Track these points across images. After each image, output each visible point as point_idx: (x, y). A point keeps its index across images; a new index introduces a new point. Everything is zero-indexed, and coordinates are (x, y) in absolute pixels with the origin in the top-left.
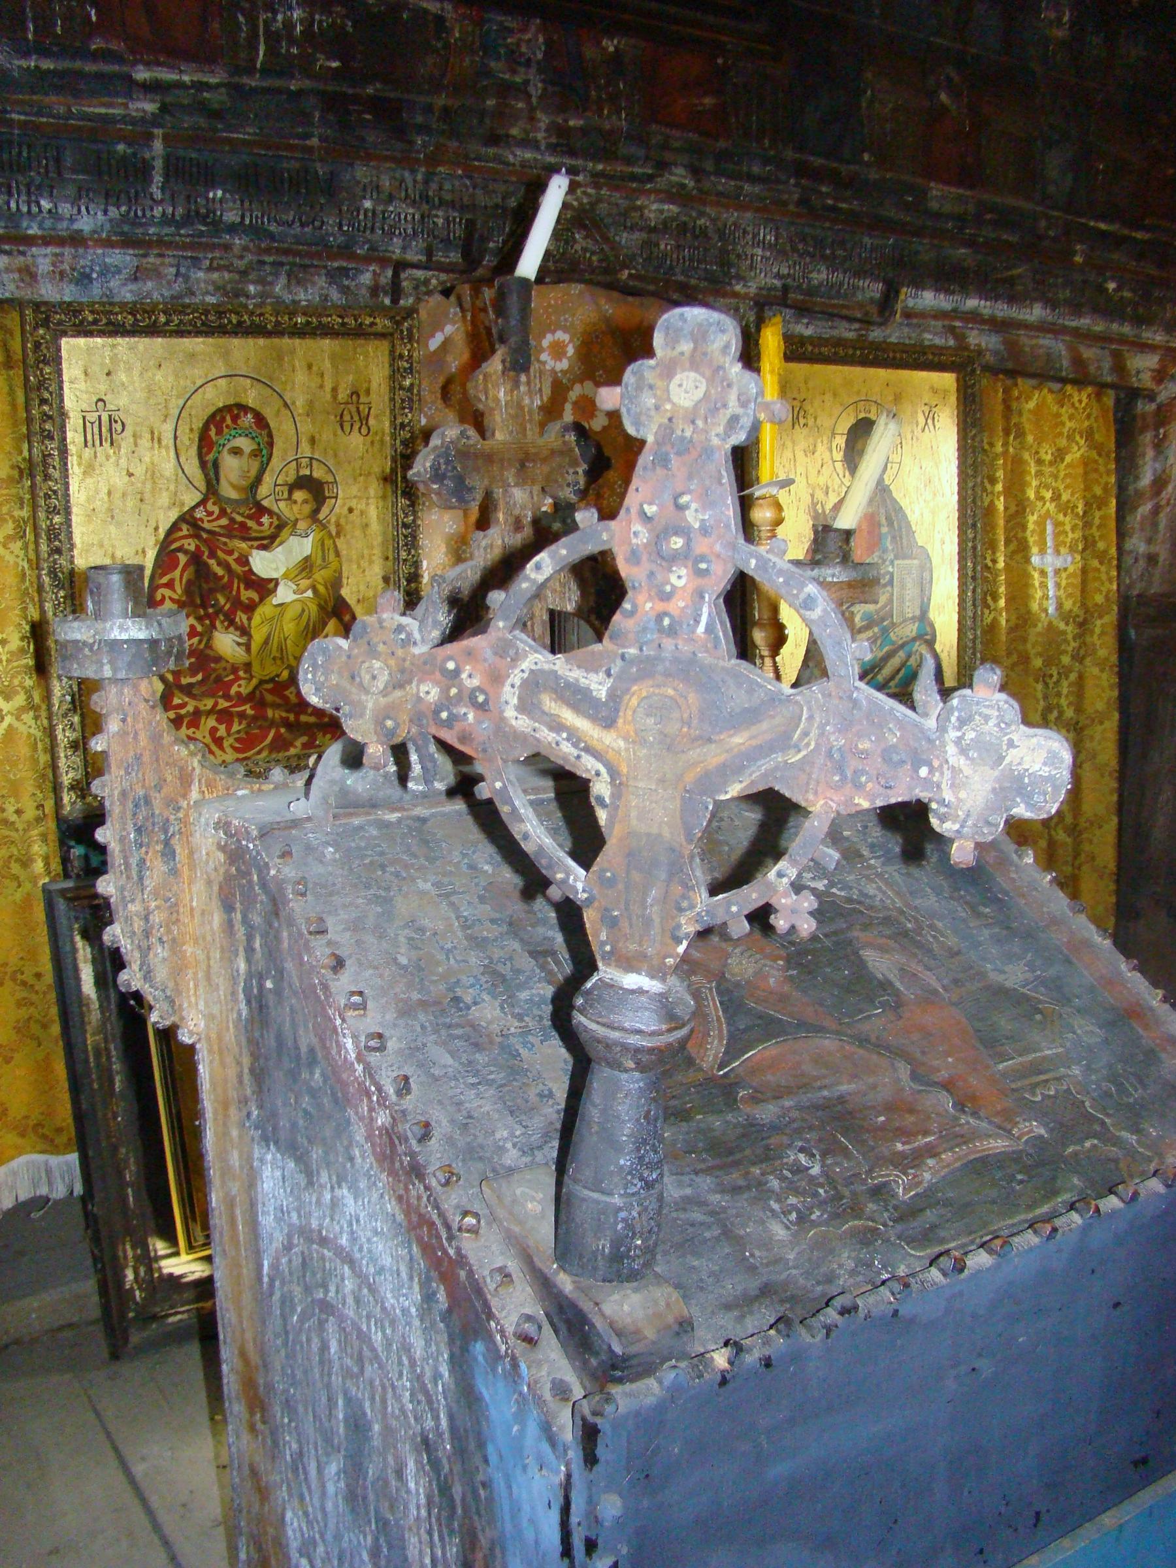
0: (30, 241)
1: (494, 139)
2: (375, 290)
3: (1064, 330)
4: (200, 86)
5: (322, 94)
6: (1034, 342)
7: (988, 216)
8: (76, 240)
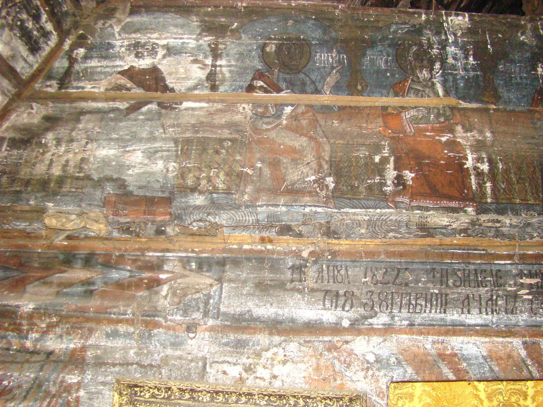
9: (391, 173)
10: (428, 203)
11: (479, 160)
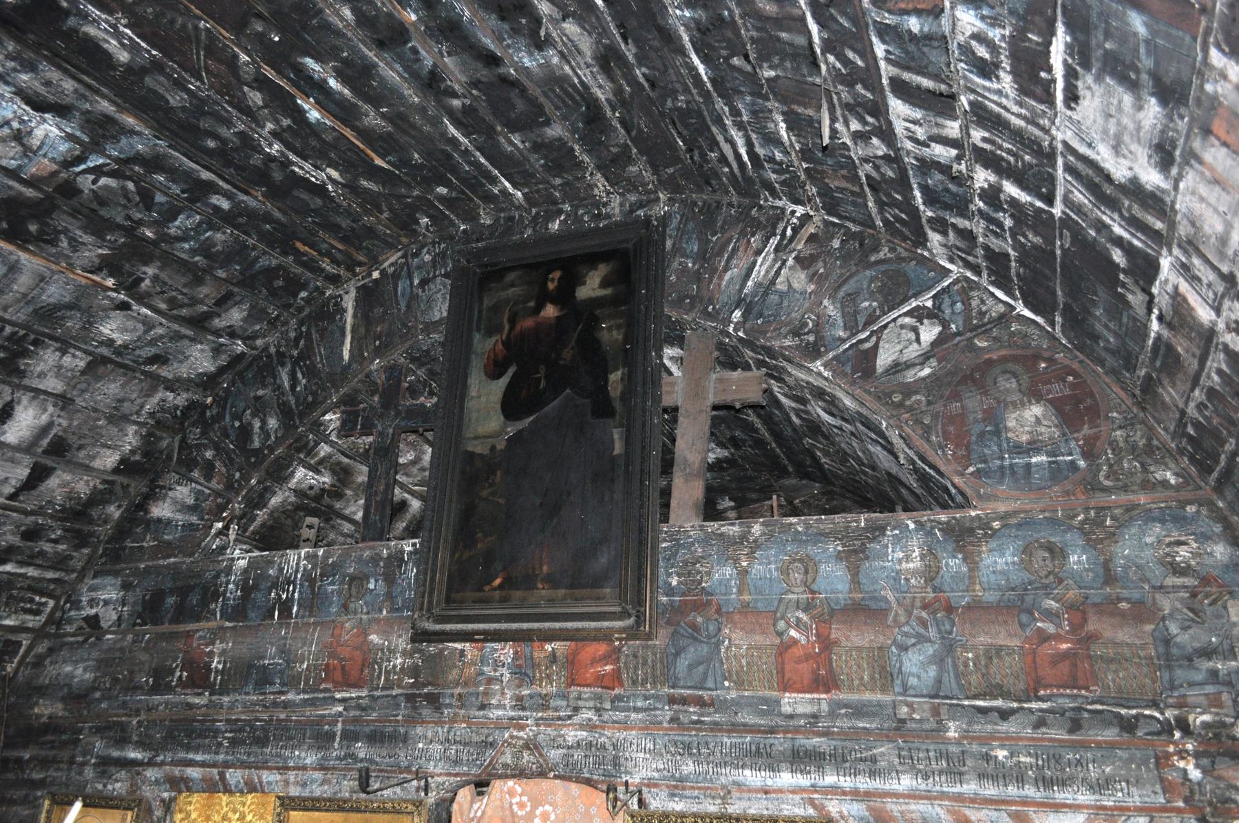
0: (288, 768)
1: (483, 707)
2: (418, 789)
3: (943, 796)
4: (359, 698)
5: (406, 695)
6: (904, 807)
7: (843, 711)
8: (304, 768)
9: (178, 674)
10: (189, 691)
11: (219, 662)
